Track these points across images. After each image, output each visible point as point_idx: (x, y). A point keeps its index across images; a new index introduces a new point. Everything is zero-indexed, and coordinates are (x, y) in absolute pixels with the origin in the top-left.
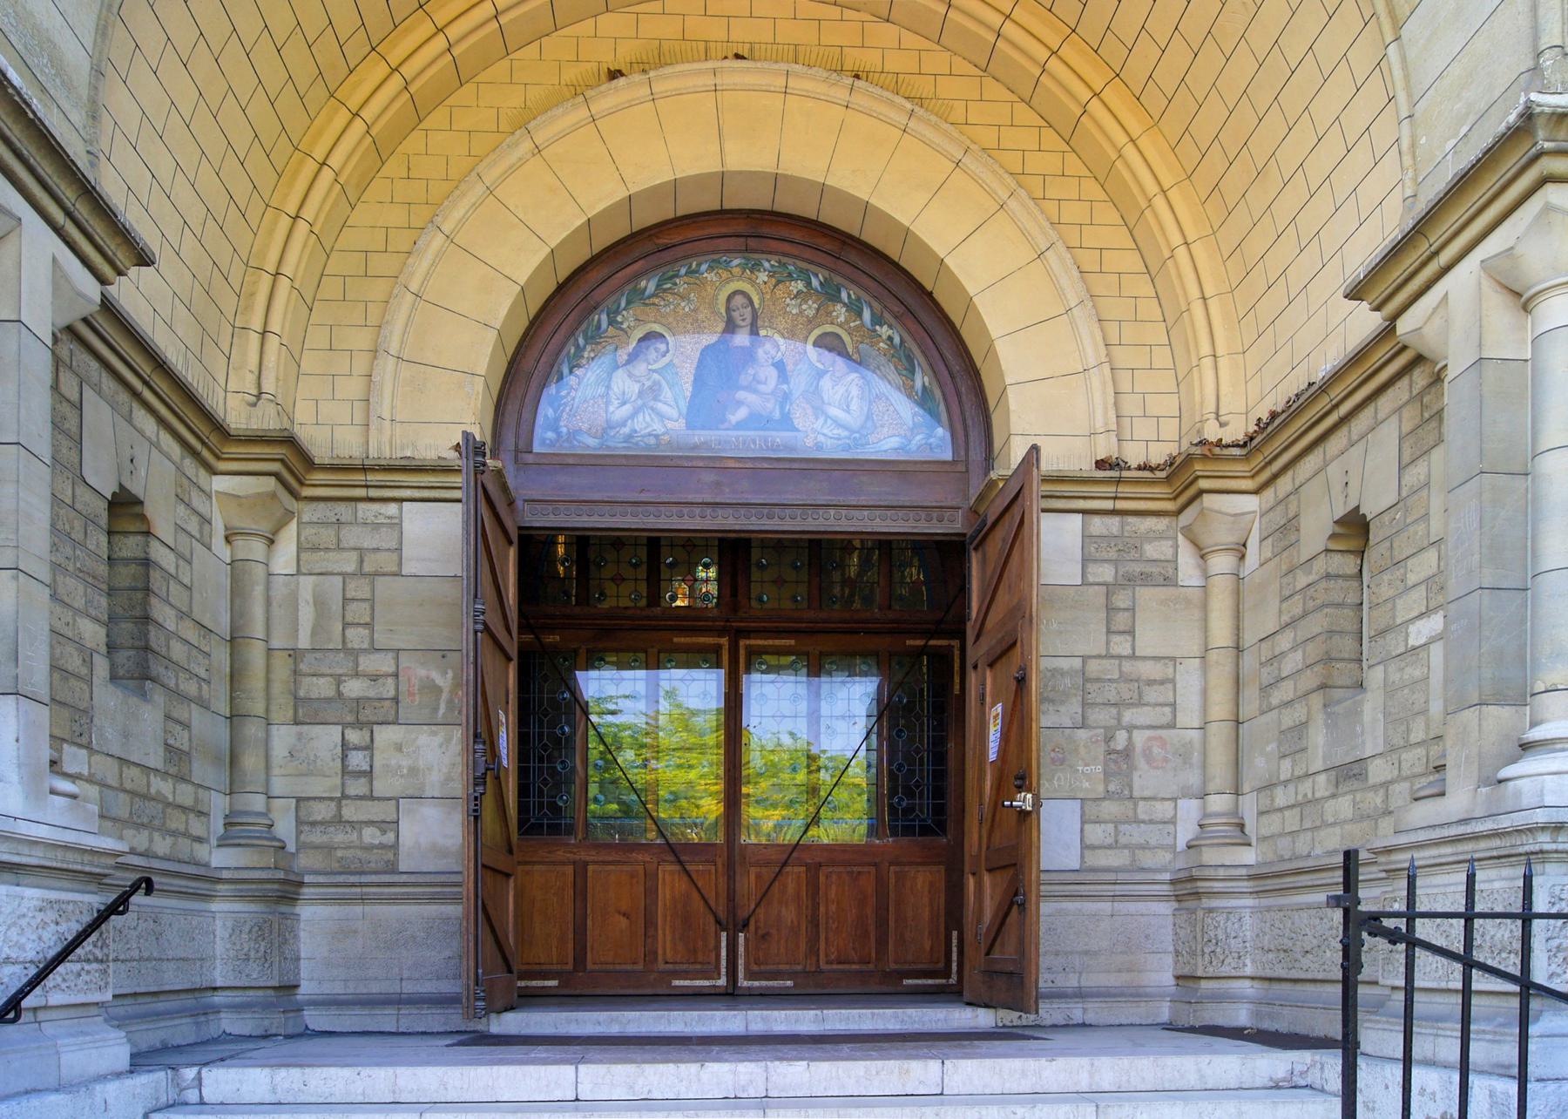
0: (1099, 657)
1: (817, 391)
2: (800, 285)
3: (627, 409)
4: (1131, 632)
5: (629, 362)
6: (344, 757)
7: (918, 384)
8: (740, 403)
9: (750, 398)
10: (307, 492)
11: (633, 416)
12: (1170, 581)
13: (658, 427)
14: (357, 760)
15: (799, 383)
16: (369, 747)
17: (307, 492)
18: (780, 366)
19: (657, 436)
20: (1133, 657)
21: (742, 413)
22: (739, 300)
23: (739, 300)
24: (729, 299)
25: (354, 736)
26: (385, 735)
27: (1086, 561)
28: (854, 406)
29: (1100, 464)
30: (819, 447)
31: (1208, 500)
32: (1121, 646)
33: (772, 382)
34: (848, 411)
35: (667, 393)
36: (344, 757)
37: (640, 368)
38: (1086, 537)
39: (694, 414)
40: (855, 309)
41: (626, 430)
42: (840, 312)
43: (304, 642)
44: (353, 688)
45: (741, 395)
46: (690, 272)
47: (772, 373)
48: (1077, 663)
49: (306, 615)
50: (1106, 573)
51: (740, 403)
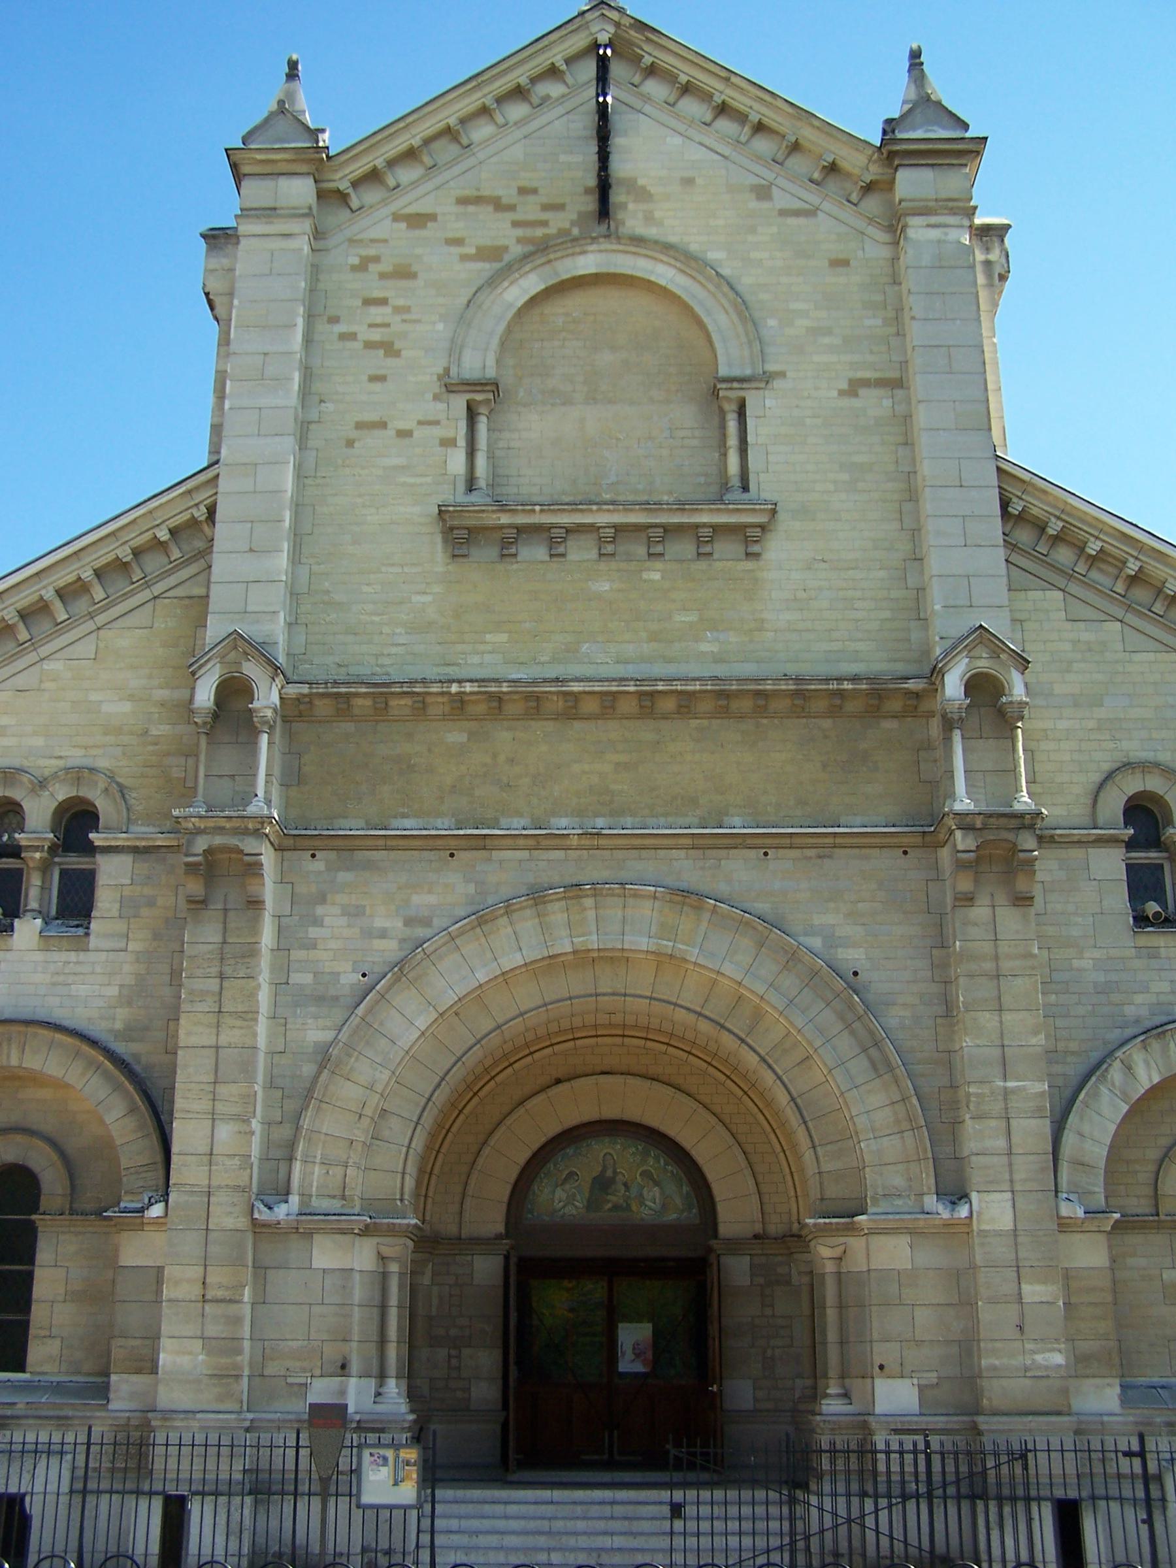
0: (759, 1316)
1: (641, 1195)
2: (634, 1149)
3: (561, 1204)
4: (772, 1306)
5: (562, 1185)
6: (449, 1361)
7: (684, 1191)
8: (609, 1201)
9: (614, 1198)
10: (436, 1252)
11: (564, 1207)
12: (788, 1283)
13: (574, 1212)
14: (454, 1362)
15: (634, 1192)
16: (459, 1357)
17: (436, 1252)
18: (625, 1185)
19: (574, 1216)
20: (773, 1316)
21: (610, 1205)
22: (608, 1157)
23: (608, 1157)
24: (605, 1155)
25: (453, 1352)
26: (466, 1352)
27: (752, 1276)
28: (657, 1201)
29: (756, 1237)
30: (642, 1219)
31: (795, 1256)
32: (768, 1311)
33: (623, 1191)
34: (655, 1203)
35: (578, 1197)
36: (449, 1361)
37: (567, 1187)
38: (752, 1266)
39: (589, 1207)
40: (657, 1159)
41: (561, 1213)
42: (651, 1161)
43: (434, 1312)
44: (453, 1332)
45: (609, 1197)
46: (588, 1146)
47: (623, 1189)
48: (750, 1319)
49: (435, 1301)
50: (761, 1280)
51: (609, 1201)
